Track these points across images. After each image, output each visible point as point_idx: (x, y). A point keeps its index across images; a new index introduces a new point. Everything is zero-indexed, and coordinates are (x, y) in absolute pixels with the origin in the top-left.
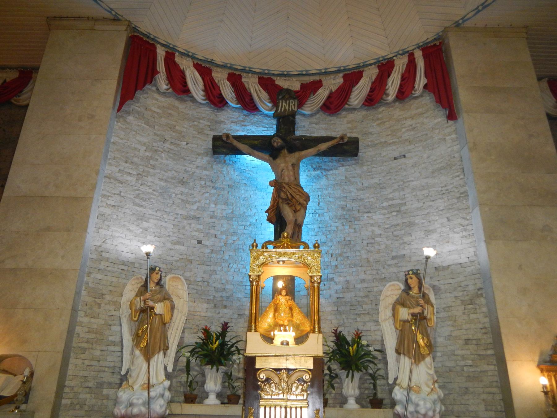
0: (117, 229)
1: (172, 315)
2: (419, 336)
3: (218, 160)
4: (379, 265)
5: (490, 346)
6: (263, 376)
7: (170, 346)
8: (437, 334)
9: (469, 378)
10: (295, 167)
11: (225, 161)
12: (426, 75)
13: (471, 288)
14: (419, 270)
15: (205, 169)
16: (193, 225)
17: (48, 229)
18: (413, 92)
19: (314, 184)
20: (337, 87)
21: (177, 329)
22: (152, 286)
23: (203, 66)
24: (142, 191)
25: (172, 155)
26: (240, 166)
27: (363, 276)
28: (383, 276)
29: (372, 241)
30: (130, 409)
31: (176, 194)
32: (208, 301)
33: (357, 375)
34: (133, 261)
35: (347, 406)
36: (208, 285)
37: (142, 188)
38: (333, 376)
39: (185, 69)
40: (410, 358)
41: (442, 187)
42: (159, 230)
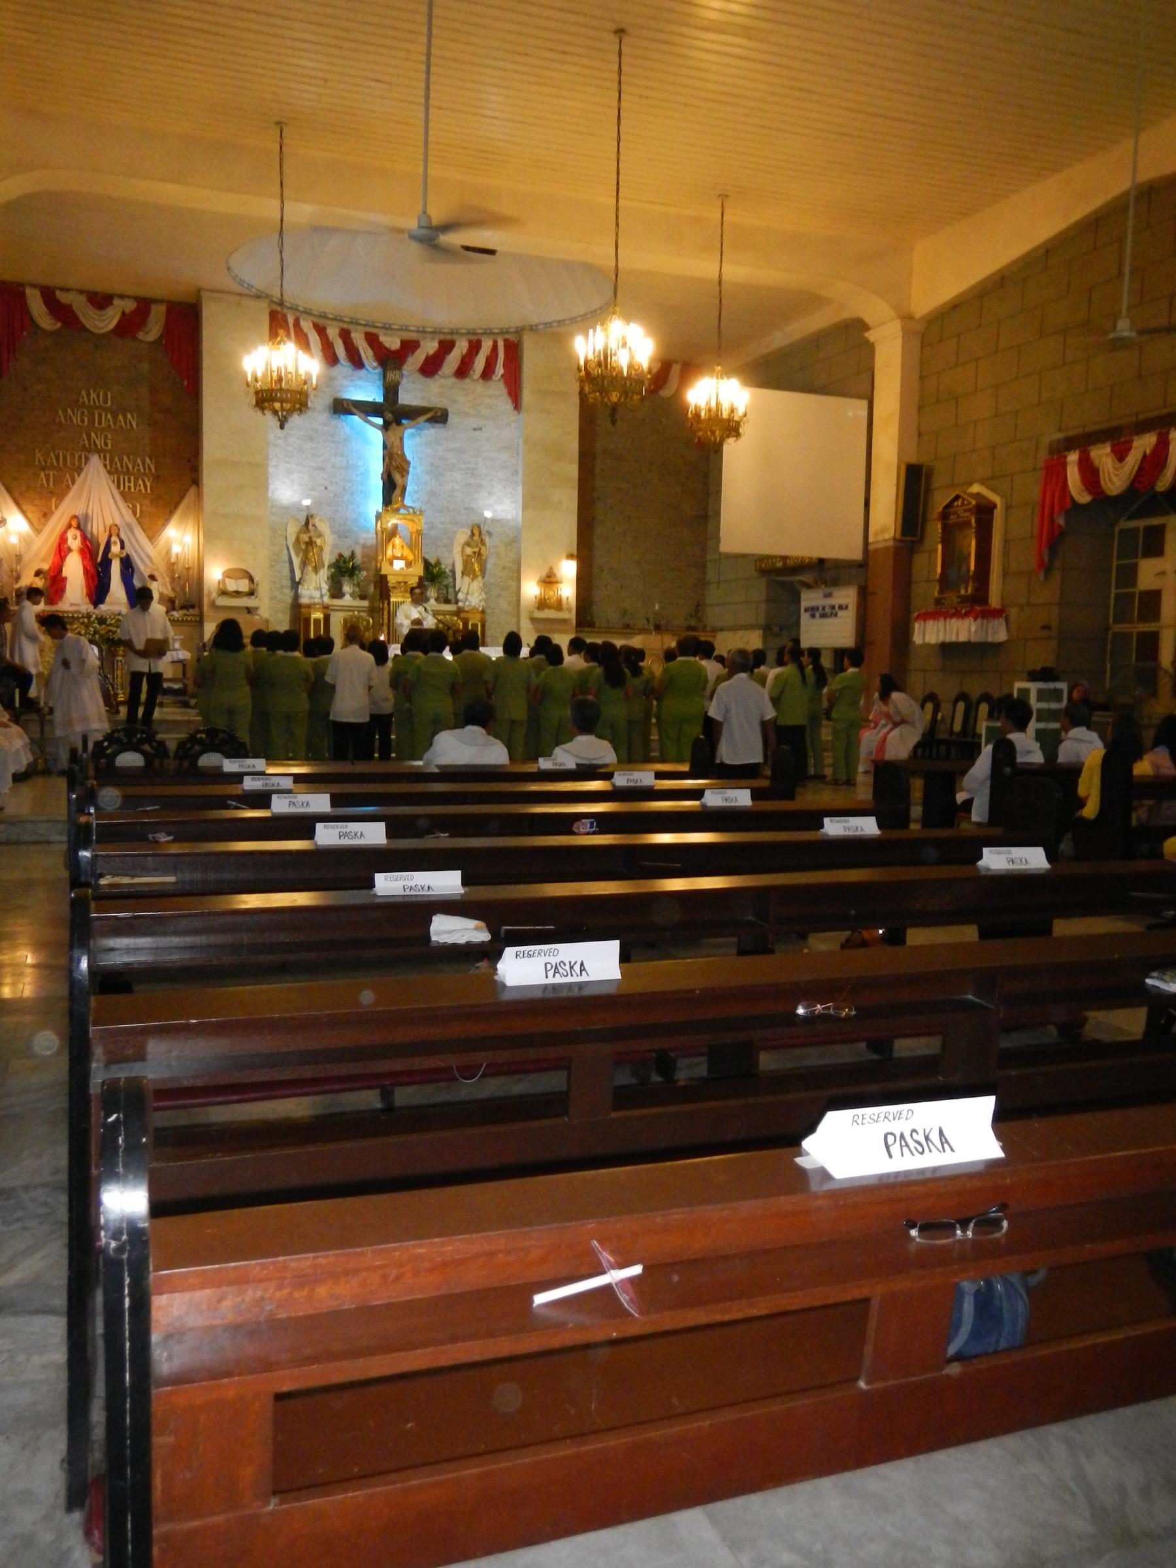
6: (390, 585)
9: (502, 589)
18: (493, 377)
22: (310, 526)
27: (443, 519)
40: (469, 577)
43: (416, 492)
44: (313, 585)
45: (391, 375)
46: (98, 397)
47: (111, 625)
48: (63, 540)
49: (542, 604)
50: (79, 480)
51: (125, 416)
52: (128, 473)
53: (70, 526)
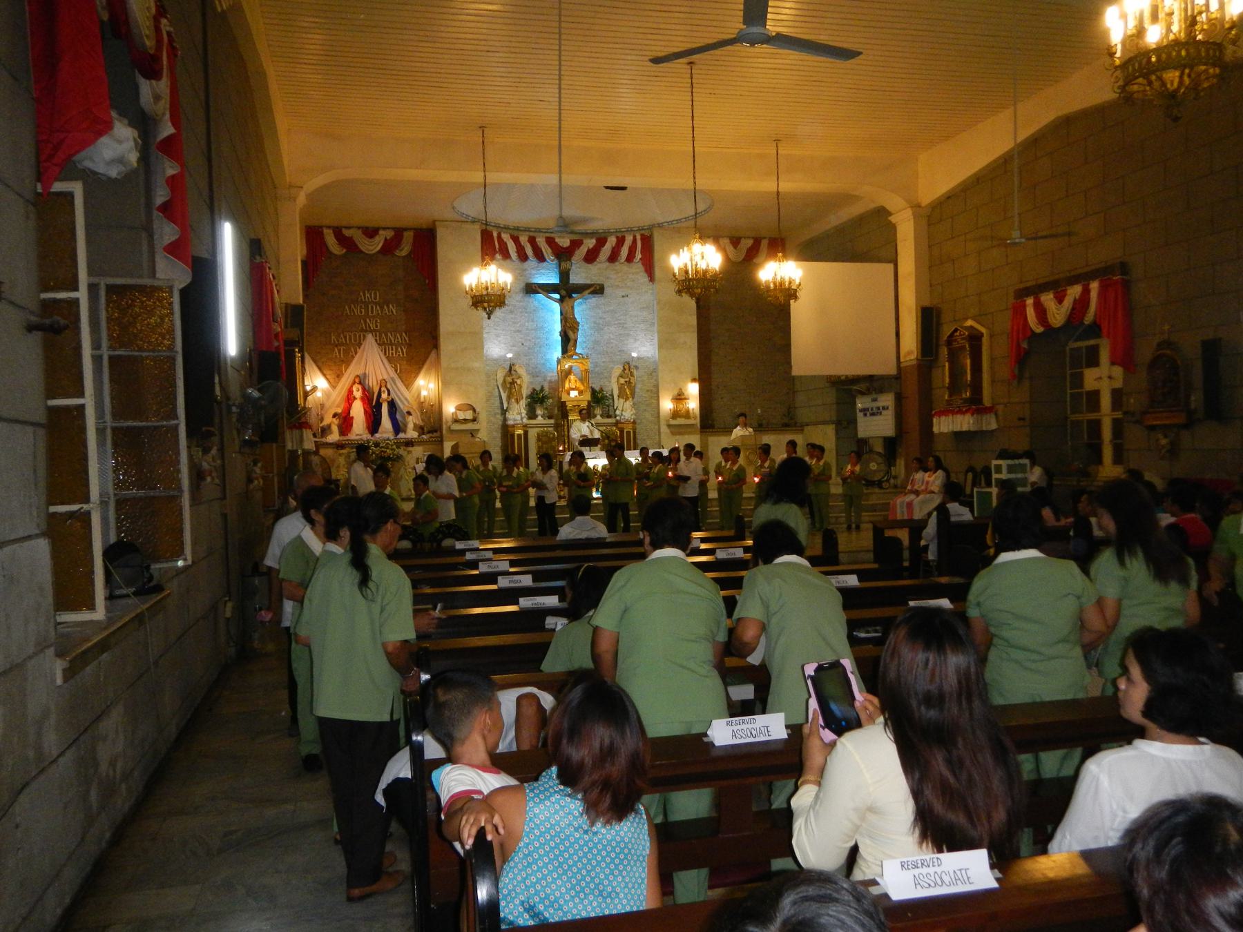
6: (568, 408)
9: (647, 405)
15: (521, 302)
17: (466, 349)
22: (512, 372)
43: (585, 342)
44: (515, 413)
45: (564, 265)
46: (371, 295)
47: (383, 447)
48: (350, 392)
49: (675, 414)
50: (360, 351)
51: (388, 307)
52: (391, 344)
53: (354, 383)
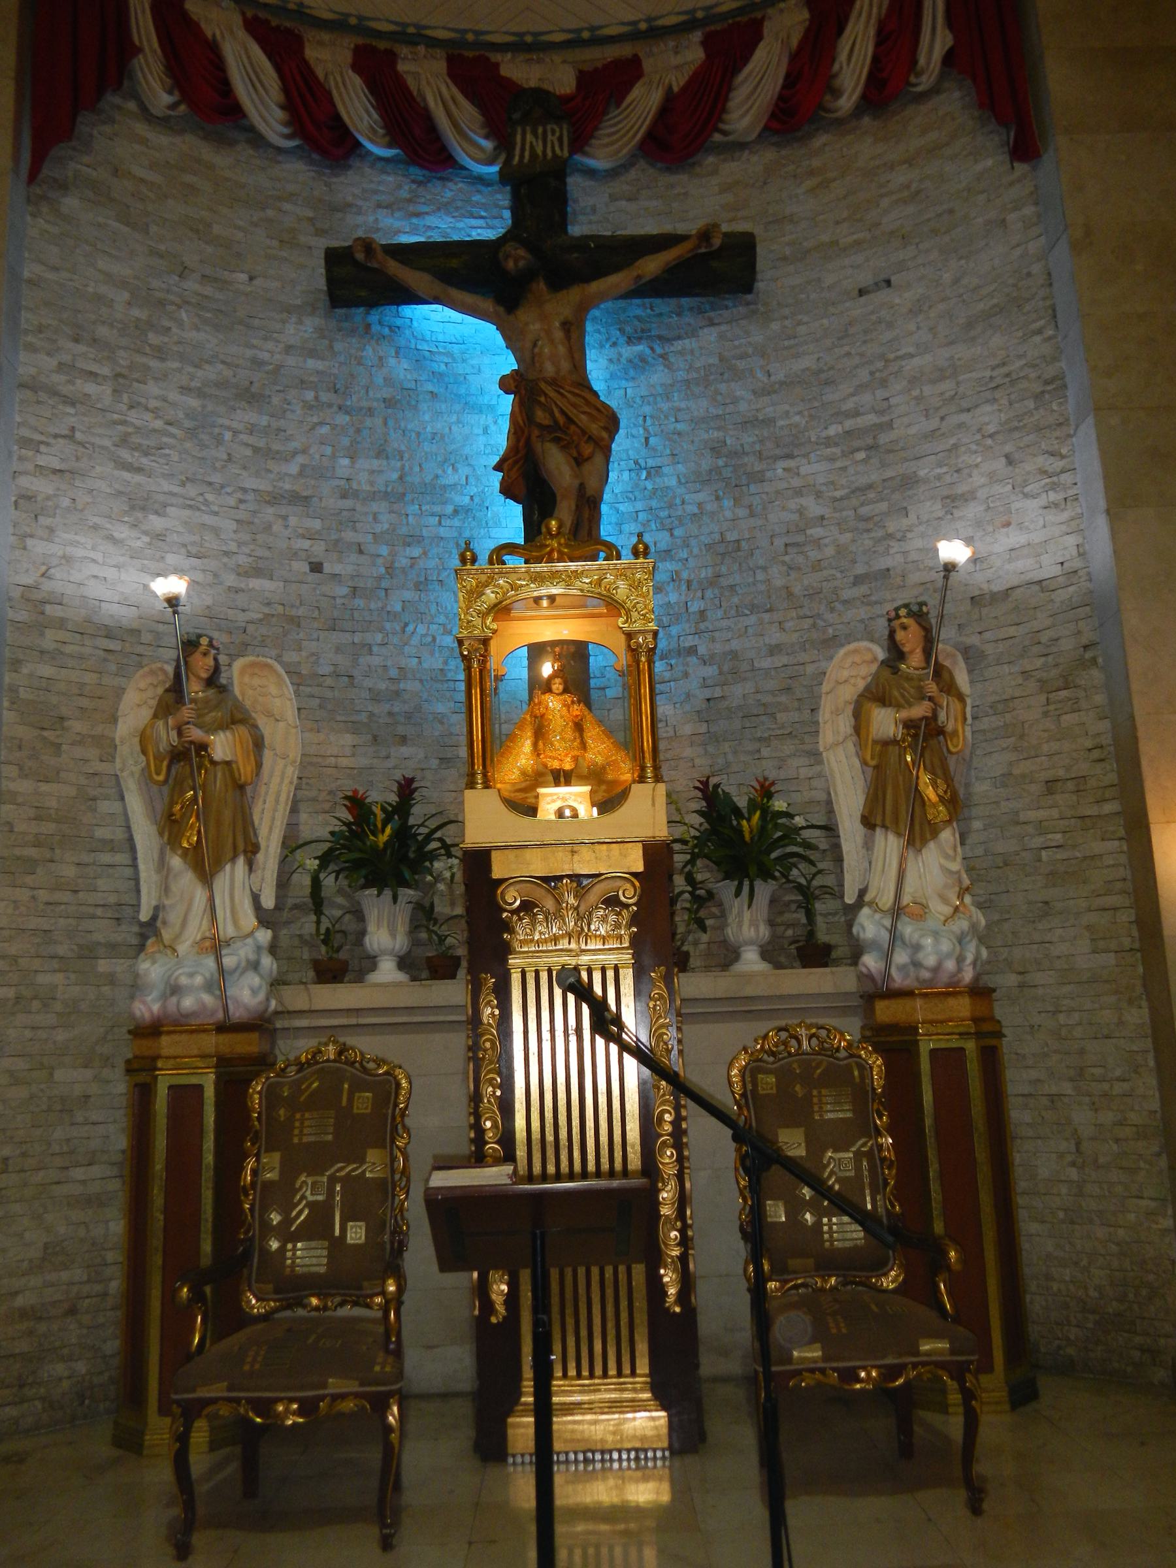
0: (77, 538)
1: (259, 765)
2: (925, 778)
3: (346, 325)
4: (820, 603)
5: (1108, 794)
6: (512, 898)
7: (263, 843)
8: (973, 773)
10: (573, 331)
11: (368, 327)
12: (951, 21)
13: (1067, 645)
14: (926, 605)
15: (313, 353)
16: (293, 521)
19: (631, 384)
20: (687, 78)
21: (277, 801)
22: (194, 689)
23: (274, 23)
24: (133, 424)
25: (209, 315)
26: (413, 341)
27: (775, 636)
28: (830, 631)
29: (800, 538)
30: (174, 999)
31: (236, 432)
32: (355, 728)
33: (764, 890)
34: (135, 625)
35: (738, 967)
36: (352, 685)
37: (133, 416)
38: (699, 897)
39: (218, 37)
40: (899, 834)
41: (993, 369)
42: (197, 538)
